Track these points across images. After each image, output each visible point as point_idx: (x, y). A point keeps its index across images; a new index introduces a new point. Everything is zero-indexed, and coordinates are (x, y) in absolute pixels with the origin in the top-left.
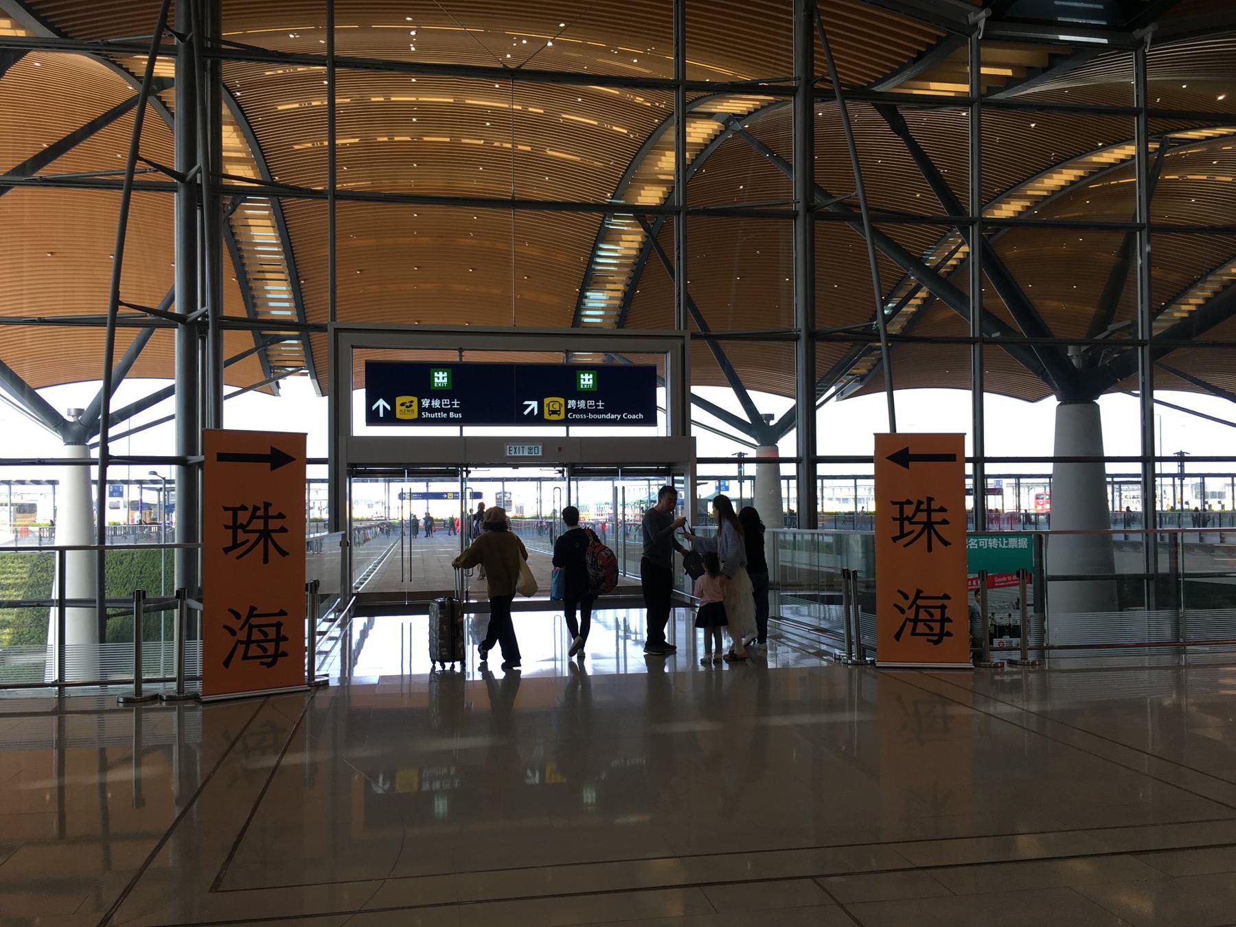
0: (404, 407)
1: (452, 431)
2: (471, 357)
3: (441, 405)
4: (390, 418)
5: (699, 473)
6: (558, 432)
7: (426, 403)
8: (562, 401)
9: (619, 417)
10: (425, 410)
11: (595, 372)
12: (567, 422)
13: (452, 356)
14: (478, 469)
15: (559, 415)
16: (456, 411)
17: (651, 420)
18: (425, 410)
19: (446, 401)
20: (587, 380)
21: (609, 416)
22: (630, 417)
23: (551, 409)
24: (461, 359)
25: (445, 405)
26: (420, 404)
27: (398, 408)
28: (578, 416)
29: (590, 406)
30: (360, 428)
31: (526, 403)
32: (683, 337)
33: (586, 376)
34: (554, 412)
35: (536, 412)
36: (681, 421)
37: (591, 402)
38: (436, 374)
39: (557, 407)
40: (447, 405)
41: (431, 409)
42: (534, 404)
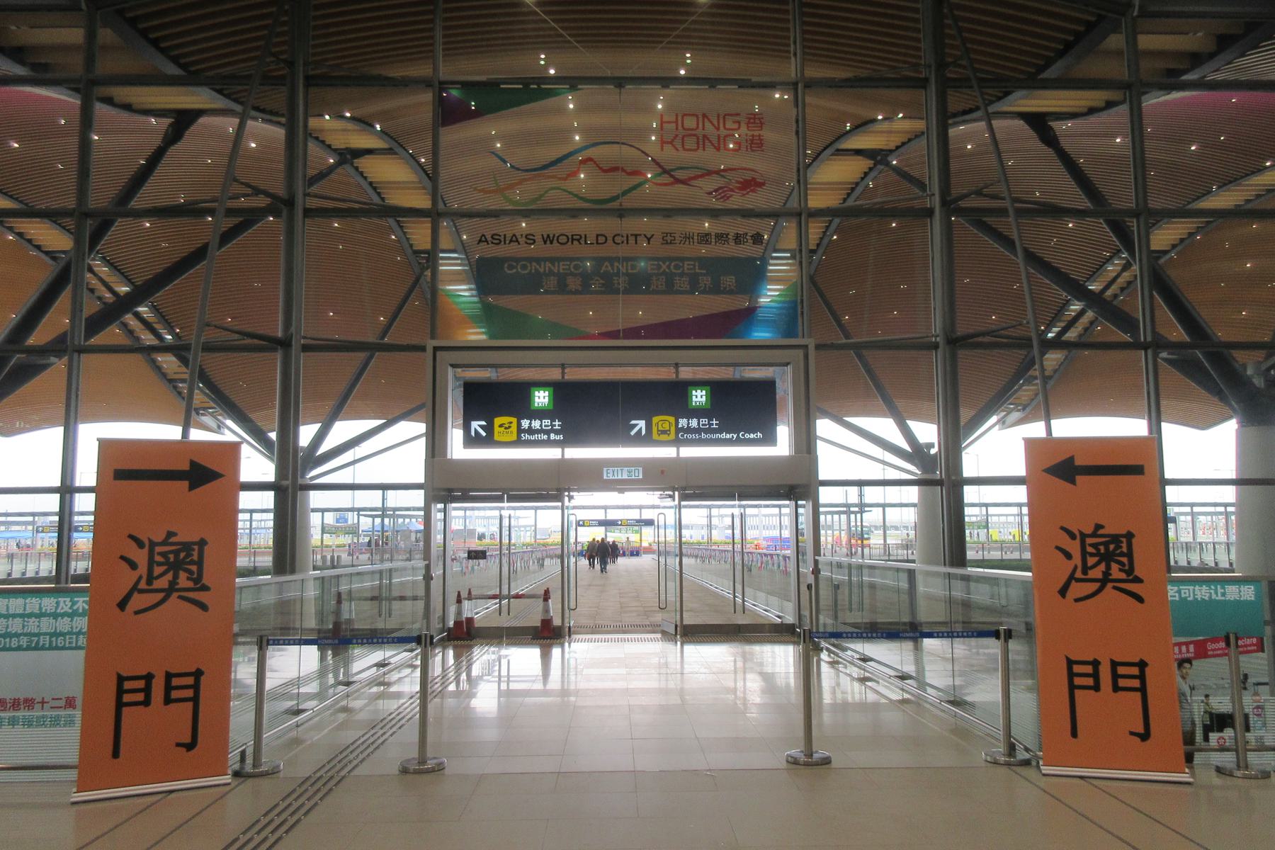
0: (502, 429)
1: (552, 453)
2: (573, 375)
3: (541, 426)
4: (488, 440)
5: (822, 500)
6: (668, 452)
7: (525, 423)
8: (672, 419)
9: (735, 436)
10: (525, 431)
11: (708, 388)
12: (677, 442)
13: (555, 374)
14: (581, 493)
15: (669, 434)
16: (557, 432)
17: (770, 439)
18: (525, 431)
19: (547, 422)
20: (699, 397)
21: (724, 436)
22: (747, 436)
23: (660, 428)
24: (563, 377)
25: (545, 426)
26: (519, 425)
27: (497, 429)
28: (690, 436)
29: (703, 425)
30: (457, 448)
31: (633, 422)
32: (806, 347)
33: (699, 393)
34: (664, 432)
35: (644, 432)
36: (806, 442)
37: (704, 421)
38: (537, 393)
39: (666, 426)
40: (548, 426)
41: (531, 431)
42: (642, 424)
